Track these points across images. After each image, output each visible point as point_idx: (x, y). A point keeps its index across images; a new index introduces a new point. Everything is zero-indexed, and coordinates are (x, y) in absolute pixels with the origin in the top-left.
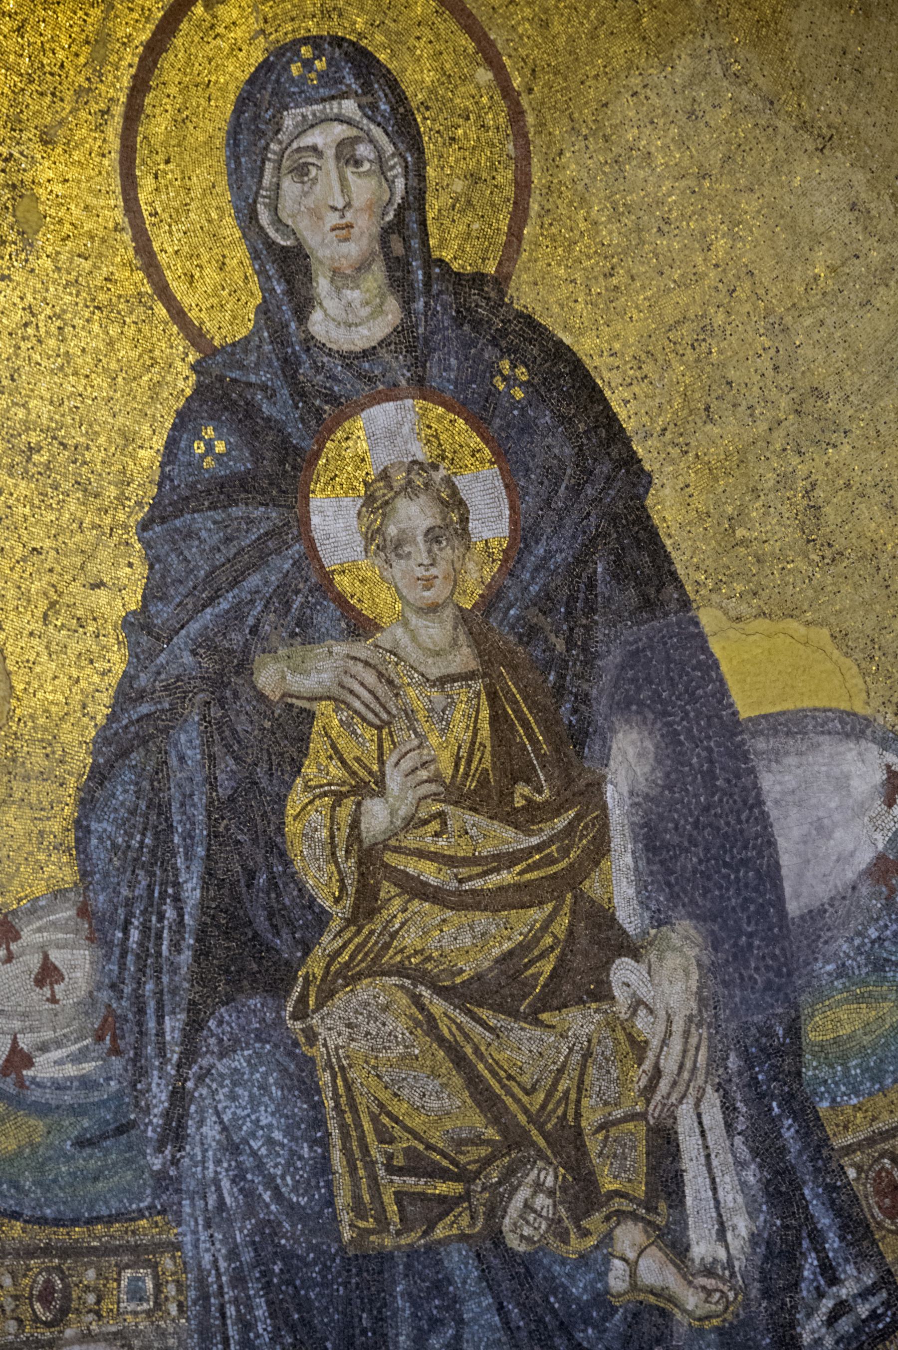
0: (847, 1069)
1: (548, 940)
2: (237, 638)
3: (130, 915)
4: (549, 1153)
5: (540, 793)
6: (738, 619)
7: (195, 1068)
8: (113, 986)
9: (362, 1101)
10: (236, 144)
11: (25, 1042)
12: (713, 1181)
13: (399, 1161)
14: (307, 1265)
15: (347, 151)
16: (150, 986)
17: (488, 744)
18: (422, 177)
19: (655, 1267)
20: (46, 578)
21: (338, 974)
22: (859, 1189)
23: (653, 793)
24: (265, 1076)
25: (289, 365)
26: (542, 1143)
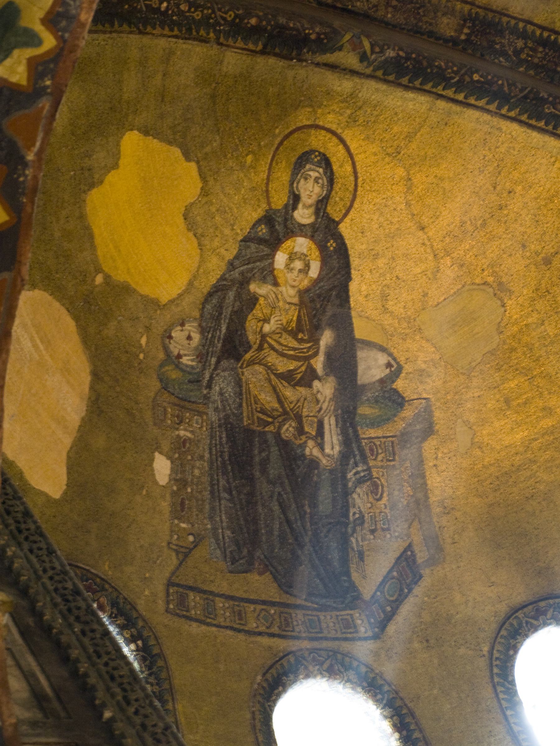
2: (249, 275)
5: (305, 336)
6: (360, 316)
8: (203, 346)
11: (182, 352)
13: (258, 409)
16: (211, 349)
18: (330, 193)
21: (252, 361)
24: (231, 379)
25: (286, 220)
26: (293, 416)
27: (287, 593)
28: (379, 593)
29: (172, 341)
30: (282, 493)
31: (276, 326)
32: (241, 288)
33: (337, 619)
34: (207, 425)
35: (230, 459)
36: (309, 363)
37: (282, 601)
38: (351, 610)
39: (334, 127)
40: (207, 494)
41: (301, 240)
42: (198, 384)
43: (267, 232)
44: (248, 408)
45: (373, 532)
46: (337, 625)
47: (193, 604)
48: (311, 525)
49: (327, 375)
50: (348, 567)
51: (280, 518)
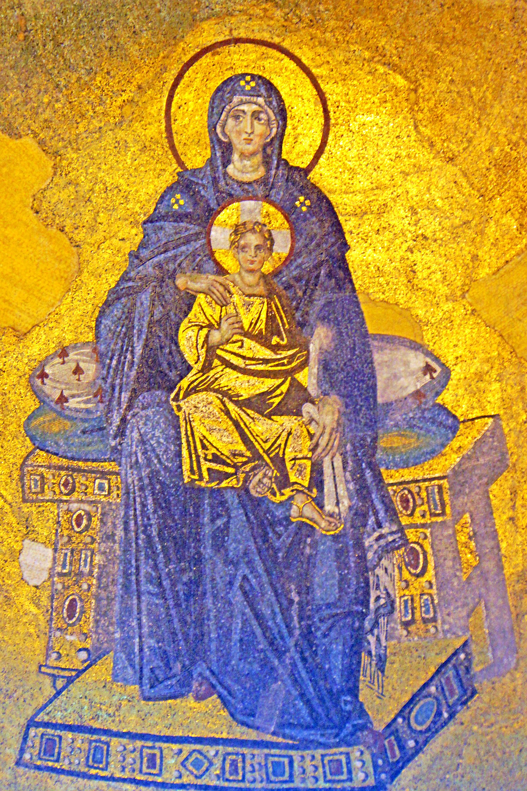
0: (394, 459)
1: (278, 392)
2: (171, 266)
3: (113, 355)
4: (271, 465)
7: (131, 412)
8: (103, 379)
9: (197, 434)
10: (214, 103)
11: (66, 393)
12: (336, 486)
14: (170, 488)
15: (256, 115)
16: (118, 381)
17: (264, 320)
18: (284, 130)
19: (310, 510)
20: (103, 234)
21: (194, 388)
22: (394, 499)
23: (330, 350)
25: (215, 180)
26: (268, 461)
27: (243, 724)
28: (400, 720)
29: (46, 381)
30: (250, 577)
31: (230, 332)
32: (161, 287)
33: (323, 761)
34: (118, 489)
35: (159, 535)
36: (293, 379)
37: (231, 737)
38: (349, 745)
39: (266, 36)
40: (117, 590)
41: (249, 204)
42: (101, 433)
43: (186, 203)
44: (191, 457)
45: (406, 625)
46: (321, 770)
47: (69, 750)
48: (301, 619)
49: (325, 394)
50: (357, 680)
51: (244, 614)
